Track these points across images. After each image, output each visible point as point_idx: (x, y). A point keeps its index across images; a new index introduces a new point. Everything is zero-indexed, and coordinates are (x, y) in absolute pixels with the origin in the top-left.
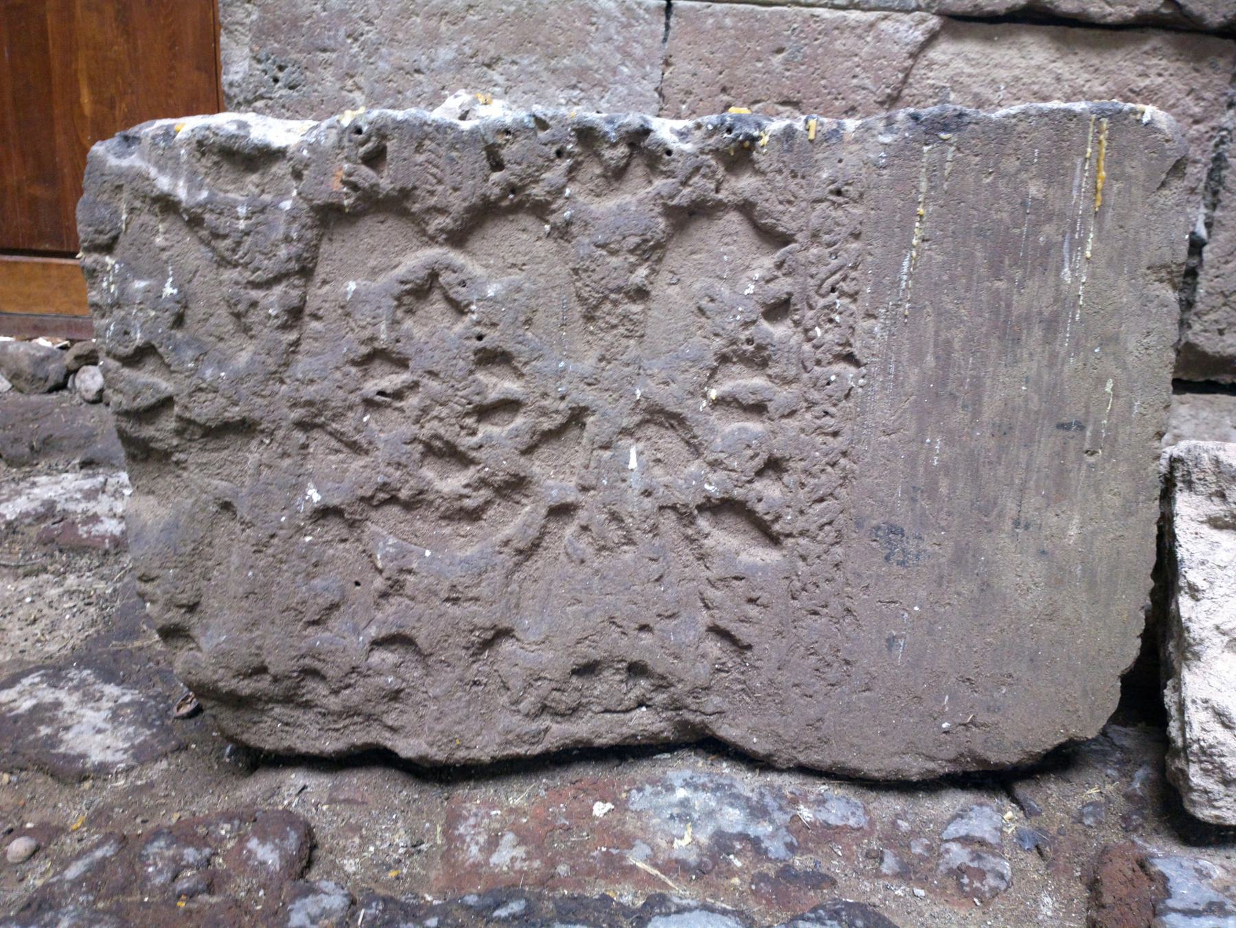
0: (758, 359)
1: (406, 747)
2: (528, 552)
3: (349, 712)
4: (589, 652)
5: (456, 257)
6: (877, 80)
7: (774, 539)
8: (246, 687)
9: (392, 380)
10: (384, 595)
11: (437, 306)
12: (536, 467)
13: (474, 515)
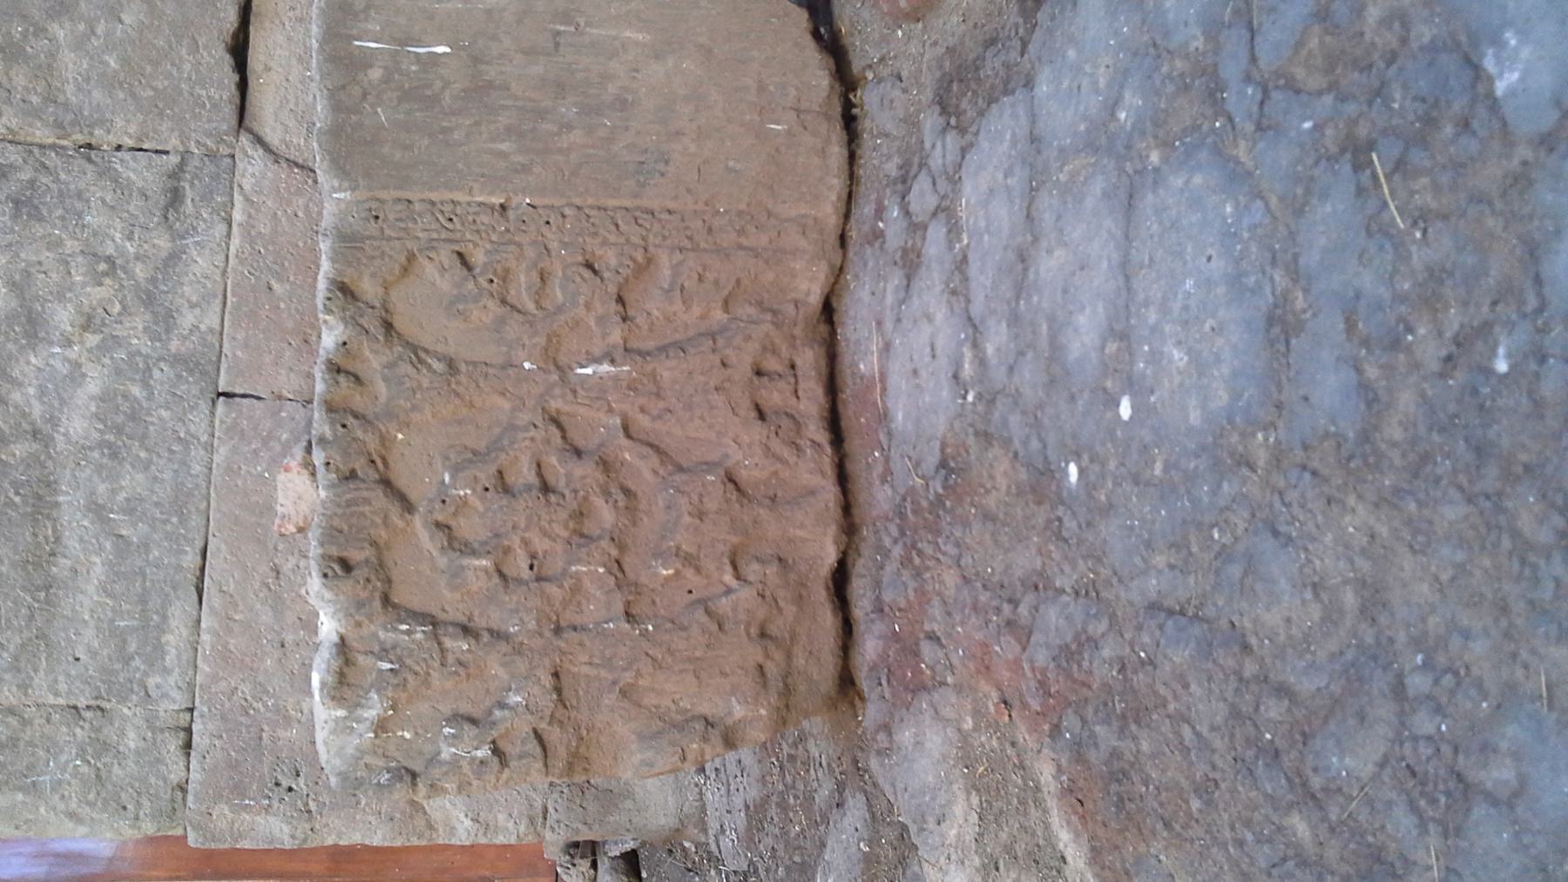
1: (831, 556)
6: (299, 192)
8: (776, 684)
10: (698, 570)
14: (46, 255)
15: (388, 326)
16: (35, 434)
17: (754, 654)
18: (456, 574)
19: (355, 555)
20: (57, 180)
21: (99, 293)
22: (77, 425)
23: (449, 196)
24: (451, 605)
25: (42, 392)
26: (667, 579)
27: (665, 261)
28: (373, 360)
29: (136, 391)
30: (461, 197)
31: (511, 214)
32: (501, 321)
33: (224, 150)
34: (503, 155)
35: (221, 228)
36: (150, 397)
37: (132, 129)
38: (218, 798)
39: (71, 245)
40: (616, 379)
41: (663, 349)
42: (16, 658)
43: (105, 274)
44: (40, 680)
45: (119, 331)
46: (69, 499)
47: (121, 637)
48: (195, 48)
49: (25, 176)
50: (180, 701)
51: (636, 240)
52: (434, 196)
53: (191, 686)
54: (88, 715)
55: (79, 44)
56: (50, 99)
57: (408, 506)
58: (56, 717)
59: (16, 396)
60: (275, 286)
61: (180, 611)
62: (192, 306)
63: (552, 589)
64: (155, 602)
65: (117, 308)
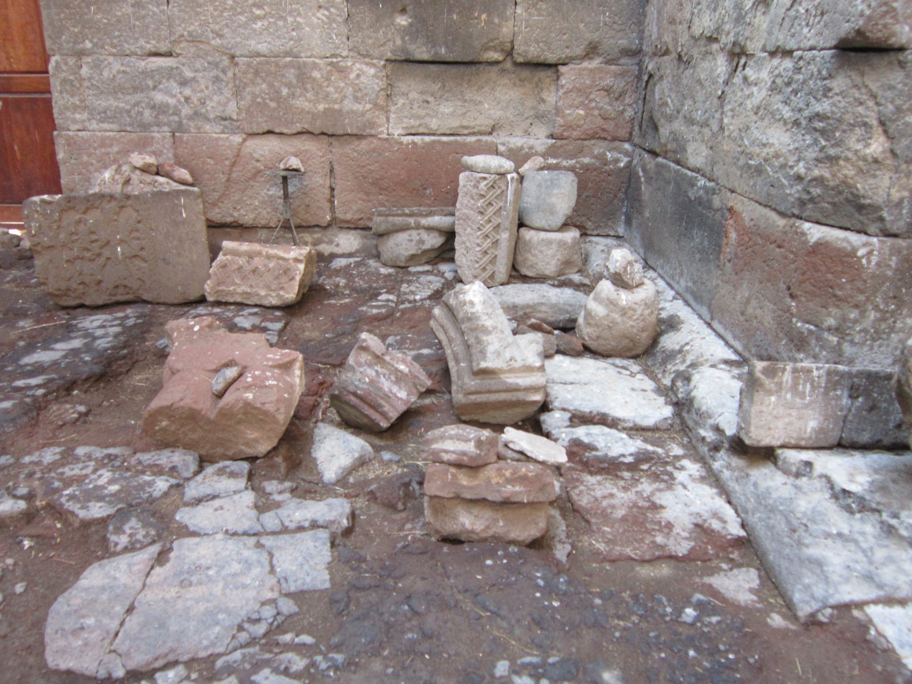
0: (137, 230)
1: (87, 303)
2: (104, 266)
3: (76, 297)
5: (84, 216)
7: (146, 262)
8: (57, 293)
9: (75, 237)
11: (82, 225)
12: (103, 251)
13: (93, 260)
14: (203, 87)
21: (195, 101)
24: (64, 223)
25: (166, 87)
29: (171, 112)
36: (170, 115)
38: (66, 140)
44: (91, 92)
46: (138, 97)
47: (105, 112)
48: (266, 122)
49: (224, 78)
50: (91, 128)
61: (114, 127)
64: (115, 120)
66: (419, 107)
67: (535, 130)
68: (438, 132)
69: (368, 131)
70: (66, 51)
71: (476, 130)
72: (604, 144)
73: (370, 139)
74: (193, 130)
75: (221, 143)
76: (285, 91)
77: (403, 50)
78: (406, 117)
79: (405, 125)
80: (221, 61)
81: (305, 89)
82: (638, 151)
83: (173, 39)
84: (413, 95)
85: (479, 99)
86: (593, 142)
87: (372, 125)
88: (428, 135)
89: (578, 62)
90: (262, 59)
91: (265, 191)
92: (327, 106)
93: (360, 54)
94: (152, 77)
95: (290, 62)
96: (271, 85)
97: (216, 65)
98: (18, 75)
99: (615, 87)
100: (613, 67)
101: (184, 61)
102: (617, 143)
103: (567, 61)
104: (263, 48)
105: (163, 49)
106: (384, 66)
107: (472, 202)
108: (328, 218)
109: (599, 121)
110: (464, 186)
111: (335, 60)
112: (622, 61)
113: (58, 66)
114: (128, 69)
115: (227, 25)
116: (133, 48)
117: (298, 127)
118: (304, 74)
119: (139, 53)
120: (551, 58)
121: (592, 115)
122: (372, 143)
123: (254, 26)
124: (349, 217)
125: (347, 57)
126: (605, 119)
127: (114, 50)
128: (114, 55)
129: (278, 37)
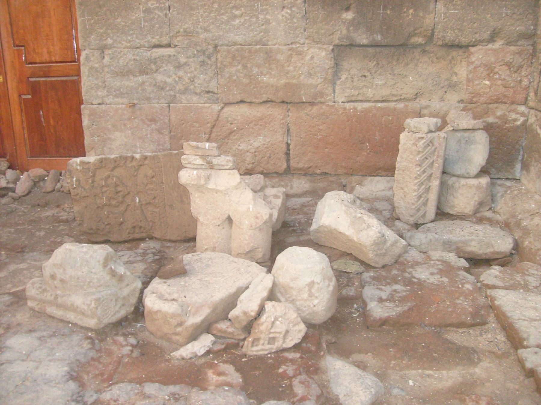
1: (112, 240)
3: (104, 235)
4: (135, 224)
10: (107, 218)
14: (193, 68)
15: (141, 165)
16: (157, 70)
17: (94, 228)
18: (102, 179)
19: (103, 164)
20: (209, 69)
22: (160, 77)
23: (163, 173)
24: (97, 178)
25: (165, 70)
26: (104, 213)
27: (157, 210)
28: (134, 163)
30: (163, 176)
31: (162, 184)
32: (143, 183)
33: (219, 101)
34: (171, 182)
35: (202, 102)
36: (167, 91)
37: (221, 83)
39: (196, 73)
40: (136, 203)
41: (142, 210)
42: (113, 70)
43: (190, 80)
45: (179, 84)
47: (119, 90)
49: (209, 62)
50: (108, 102)
51: (160, 205)
52: (163, 172)
53: (111, 104)
54: (104, 85)
55: (237, 71)
56: (225, 66)
57: (112, 170)
58: (103, 79)
59: (164, 65)
60: (193, 113)
62: (186, 98)
63: (101, 195)
65: (184, 83)
66: (358, 80)
67: (448, 96)
68: (373, 100)
69: (319, 99)
70: (93, 47)
71: (403, 98)
72: (504, 107)
73: (320, 105)
74: (184, 102)
75: (204, 111)
76: (255, 70)
77: (347, 38)
78: (348, 88)
79: (346, 94)
80: (207, 49)
81: (271, 69)
82: (532, 112)
83: (171, 34)
84: (354, 71)
85: (405, 73)
86: (496, 105)
87: (322, 94)
88: (365, 101)
89: (484, 44)
90: (239, 47)
91: (237, 146)
92: (287, 81)
93: (314, 41)
94: (155, 63)
95: (260, 49)
96: (245, 67)
97: (203, 52)
98: (55, 64)
99: (513, 64)
100: (512, 48)
101: (180, 50)
102: (514, 106)
103: (476, 43)
104: (239, 39)
105: (165, 41)
106: (333, 50)
107: (411, 156)
108: (285, 166)
109: (502, 90)
110: (405, 144)
111: (294, 46)
112: (520, 43)
113: (87, 58)
114: (138, 58)
115: (213, 23)
116: (142, 42)
117: (264, 97)
118: (271, 57)
119: (147, 46)
120: (464, 41)
121: (496, 85)
122: (321, 108)
123: (233, 23)
124: (301, 165)
125: (304, 44)
126: (506, 87)
127: (129, 44)
128: (128, 48)
129: (252, 30)
